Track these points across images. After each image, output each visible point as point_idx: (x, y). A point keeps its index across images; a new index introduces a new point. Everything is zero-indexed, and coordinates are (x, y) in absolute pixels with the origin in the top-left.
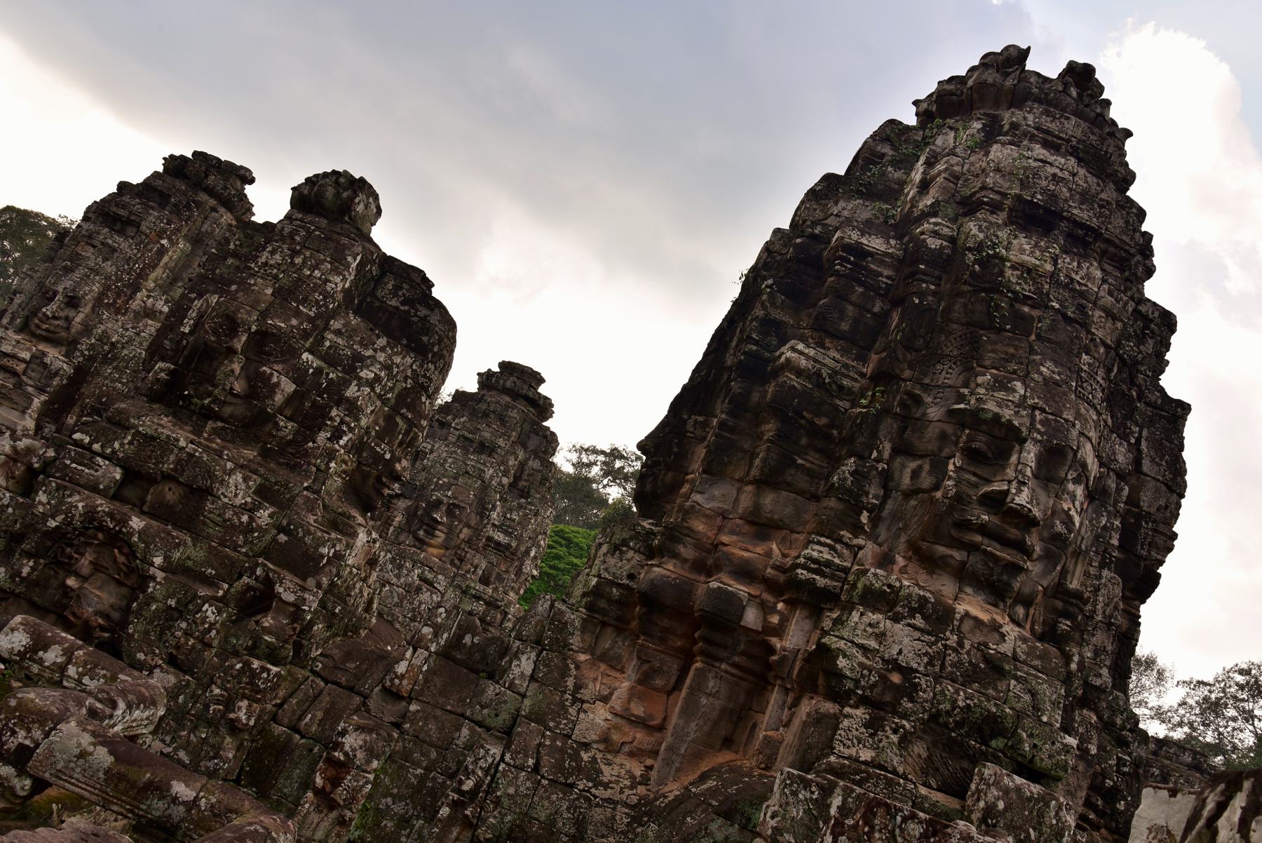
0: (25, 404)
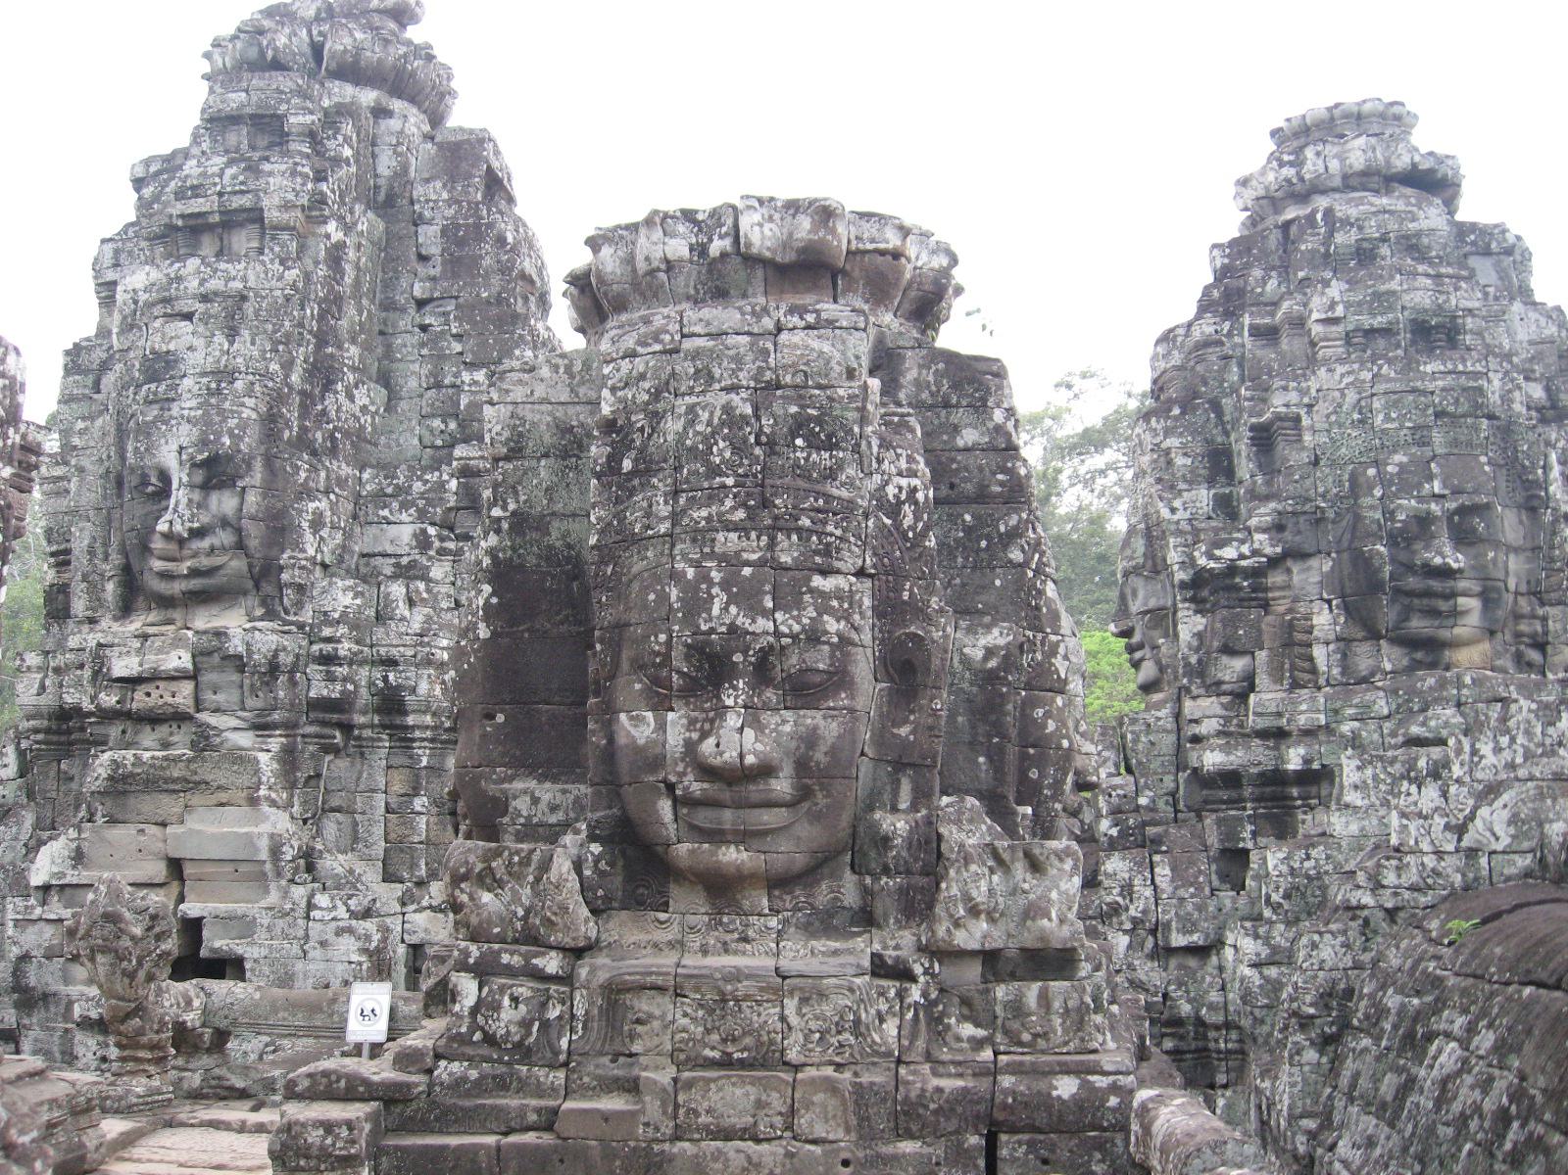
0: (245, 780)
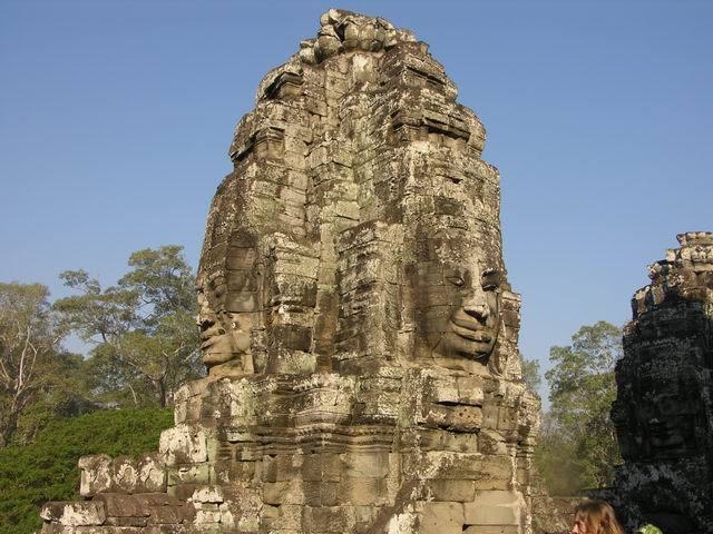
0: (506, 474)
